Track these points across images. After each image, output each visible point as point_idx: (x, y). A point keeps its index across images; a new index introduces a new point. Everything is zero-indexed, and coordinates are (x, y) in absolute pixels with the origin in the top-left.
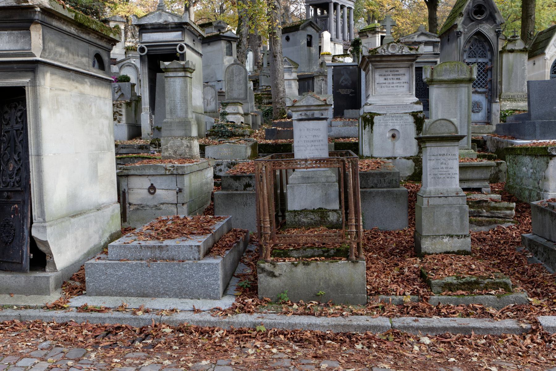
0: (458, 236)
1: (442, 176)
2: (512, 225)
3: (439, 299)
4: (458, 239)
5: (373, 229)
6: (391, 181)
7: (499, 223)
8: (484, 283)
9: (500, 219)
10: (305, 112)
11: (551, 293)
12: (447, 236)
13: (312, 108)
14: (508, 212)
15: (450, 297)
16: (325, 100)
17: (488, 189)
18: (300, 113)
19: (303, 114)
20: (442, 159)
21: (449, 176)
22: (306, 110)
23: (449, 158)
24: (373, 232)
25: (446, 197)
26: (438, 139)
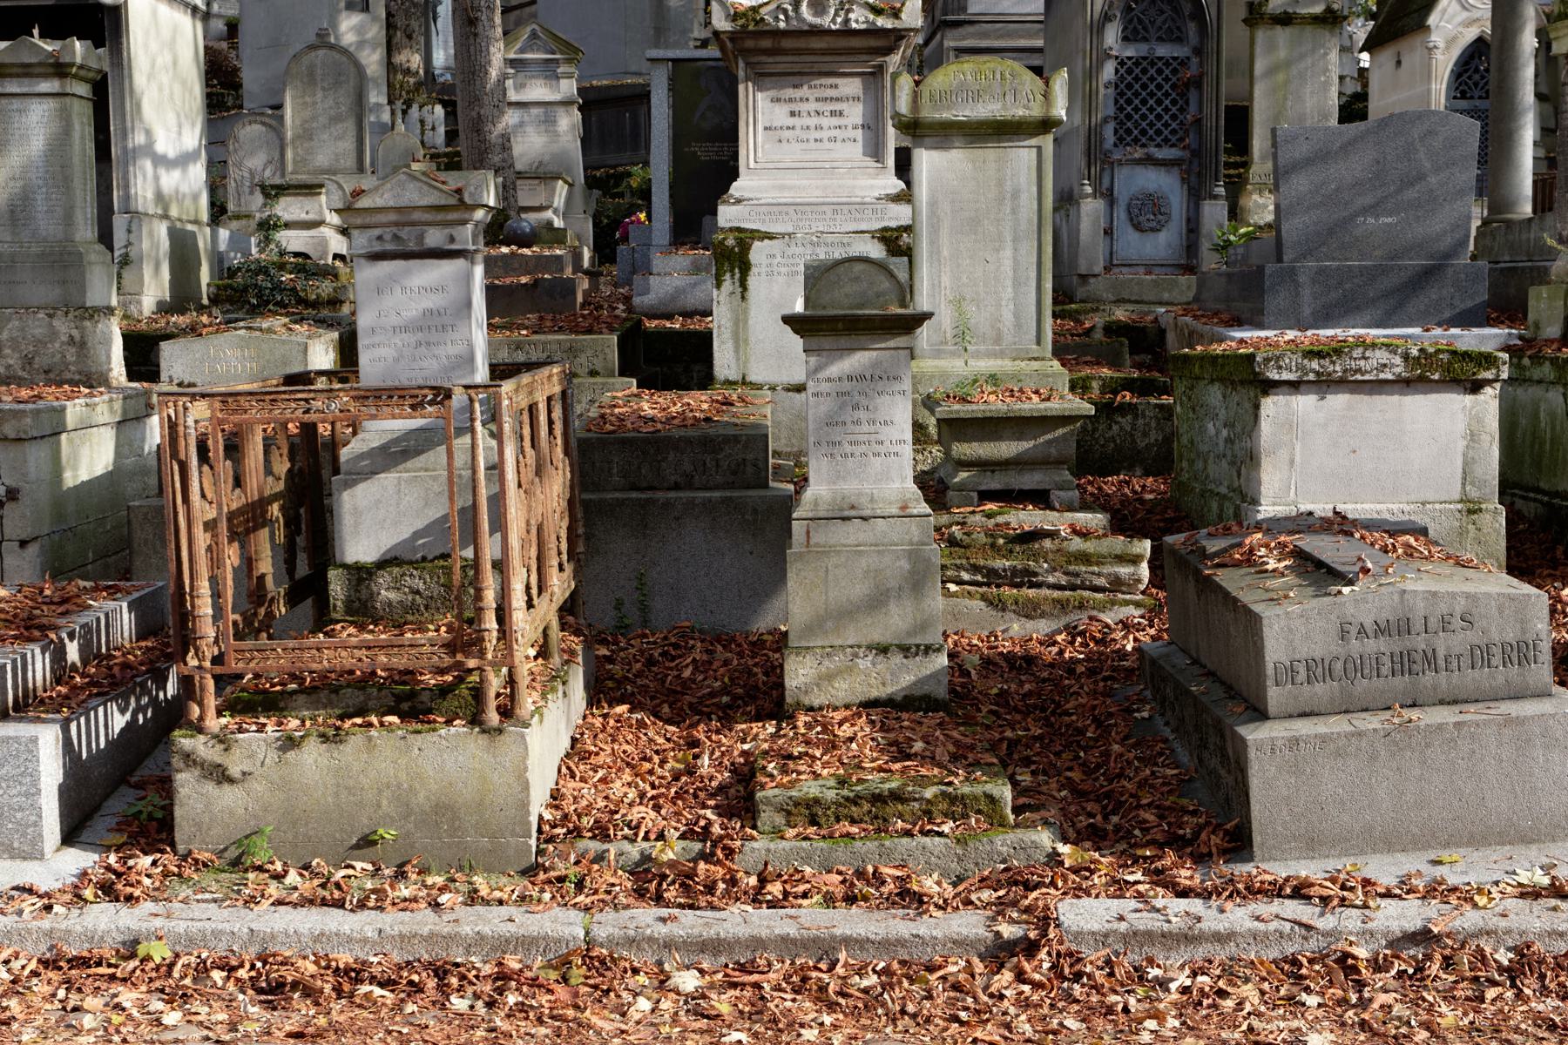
0: (905, 650)
1: (858, 450)
2: (1137, 612)
3: (768, 850)
4: (906, 657)
5: (675, 628)
6: (738, 465)
7: (1094, 608)
8: (922, 798)
9: (1100, 596)
10: (394, 229)
11: (1142, 830)
12: (869, 648)
13: (416, 216)
14: (1124, 571)
15: (805, 844)
16: (459, 191)
17: (1070, 493)
18: (377, 232)
19: (388, 237)
20: (856, 393)
21: (879, 448)
22: (397, 224)
24: (673, 640)
25: (864, 519)
26: (840, 325)
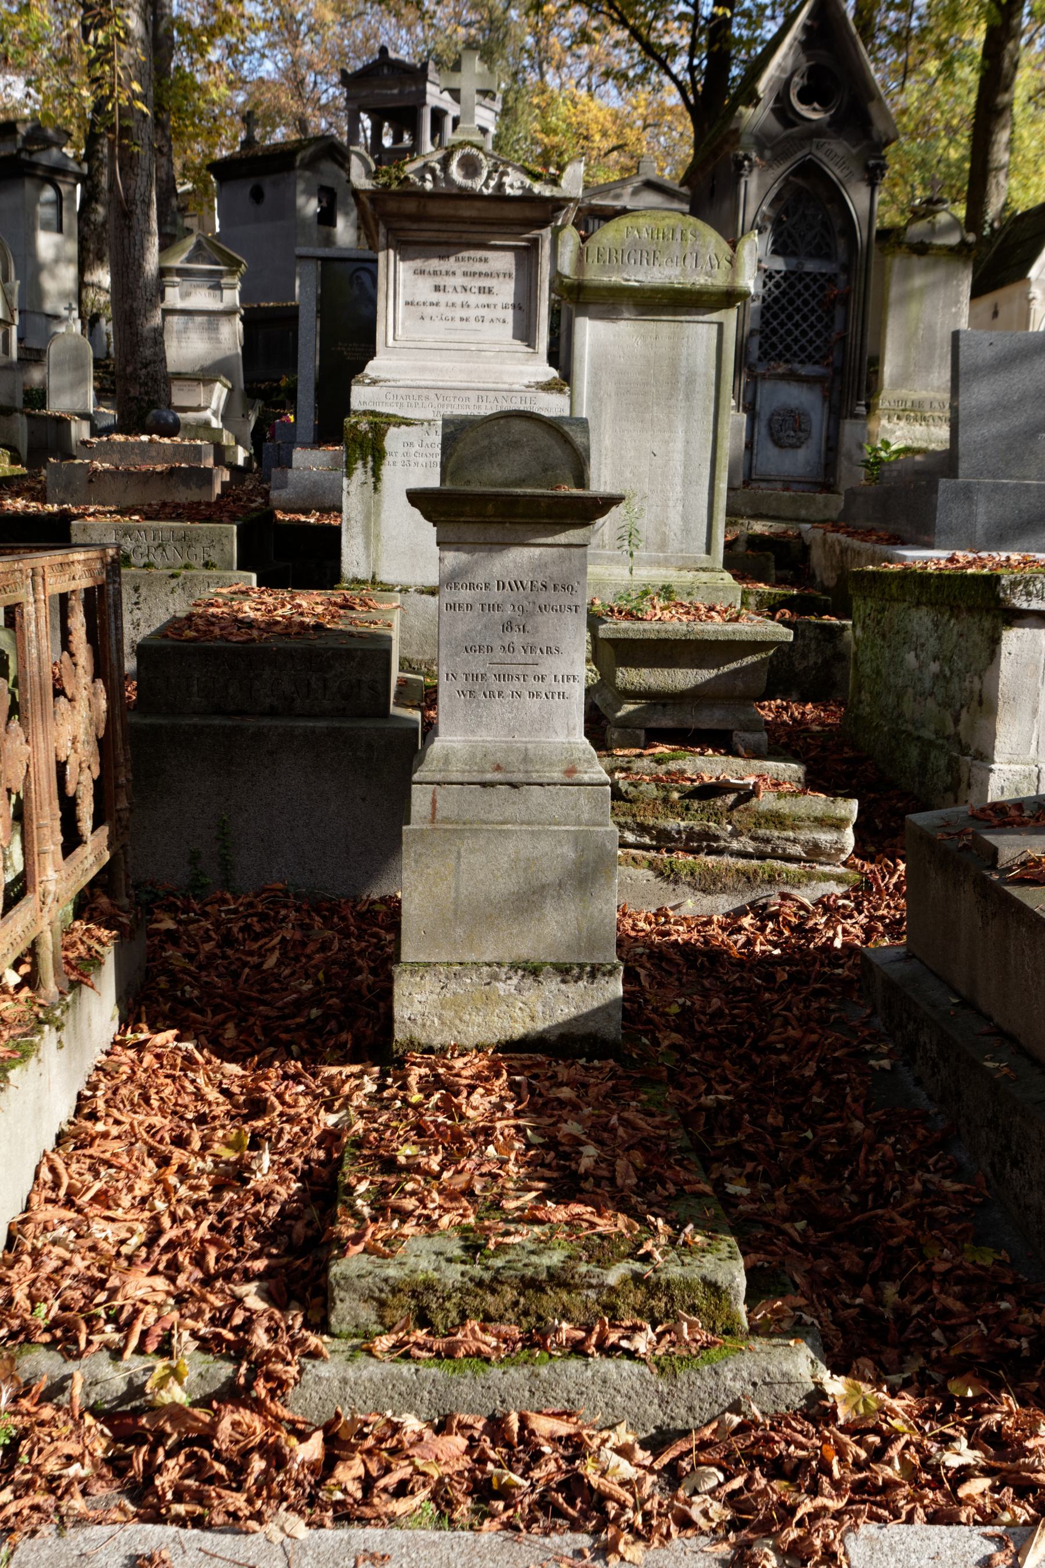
0: (564, 971)
1: (509, 687)
2: (839, 890)
3: (345, 1381)
4: (564, 981)
5: (264, 891)
7: (787, 883)
8: (602, 1285)
9: (793, 867)
11: (945, 1329)
12: (514, 967)
14: (825, 837)
15: (406, 1369)
17: (757, 736)
23: (542, 602)
24: (260, 908)
25: (513, 785)
